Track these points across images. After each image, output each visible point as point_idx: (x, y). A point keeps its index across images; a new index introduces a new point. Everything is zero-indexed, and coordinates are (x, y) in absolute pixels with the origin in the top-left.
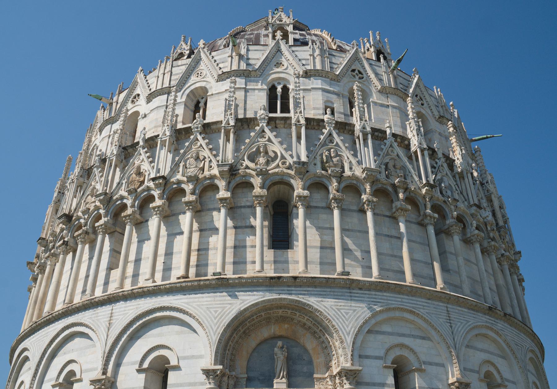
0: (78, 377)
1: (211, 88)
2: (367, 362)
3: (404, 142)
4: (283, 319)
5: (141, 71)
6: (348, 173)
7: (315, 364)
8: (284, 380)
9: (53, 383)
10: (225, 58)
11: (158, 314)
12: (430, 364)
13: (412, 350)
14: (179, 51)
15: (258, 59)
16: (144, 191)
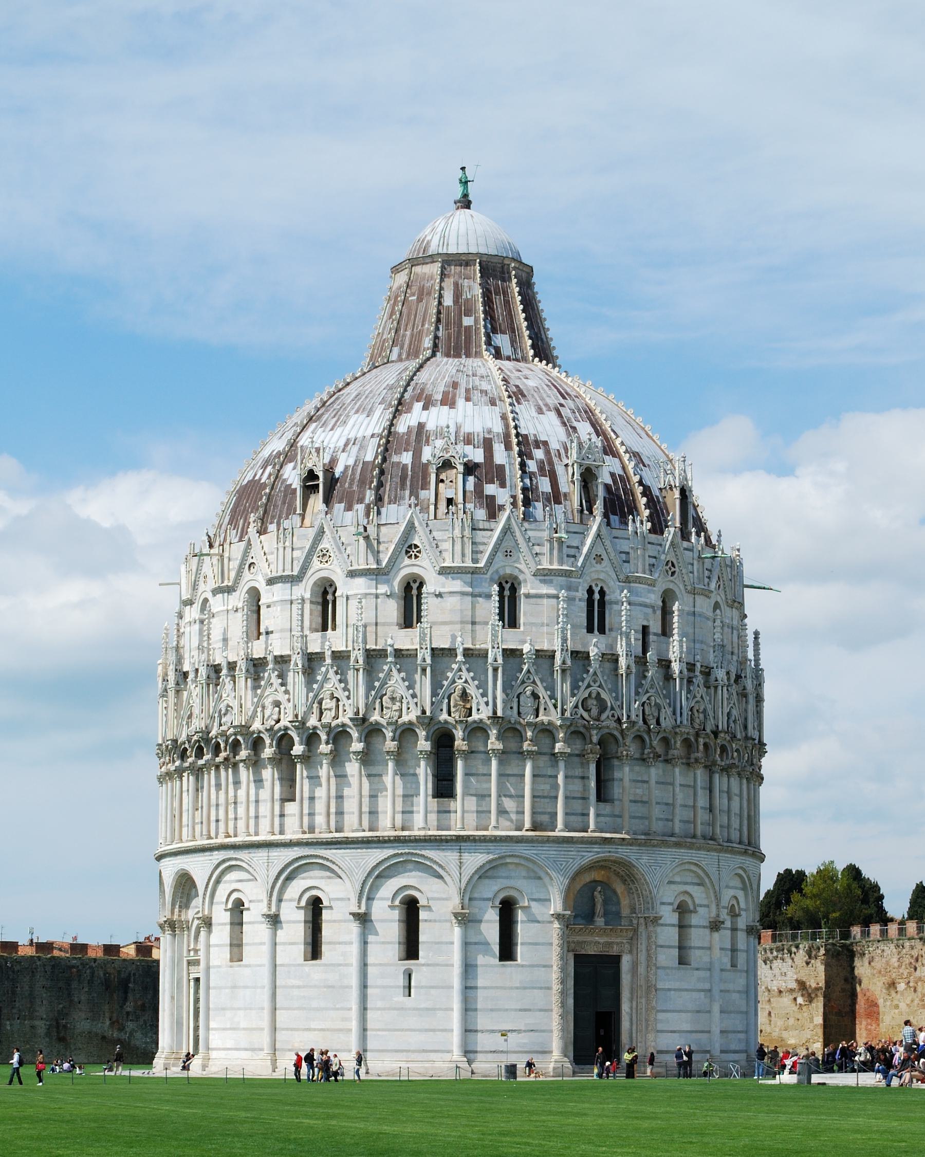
0: (422, 902)
1: (525, 581)
2: (663, 907)
3: (707, 672)
4: (603, 867)
5: (416, 505)
6: (663, 724)
7: (622, 905)
8: (603, 919)
9: (390, 904)
10: (540, 538)
11: (508, 861)
12: (701, 906)
13: (691, 896)
14: (447, 456)
15: (577, 548)
16: (475, 722)
